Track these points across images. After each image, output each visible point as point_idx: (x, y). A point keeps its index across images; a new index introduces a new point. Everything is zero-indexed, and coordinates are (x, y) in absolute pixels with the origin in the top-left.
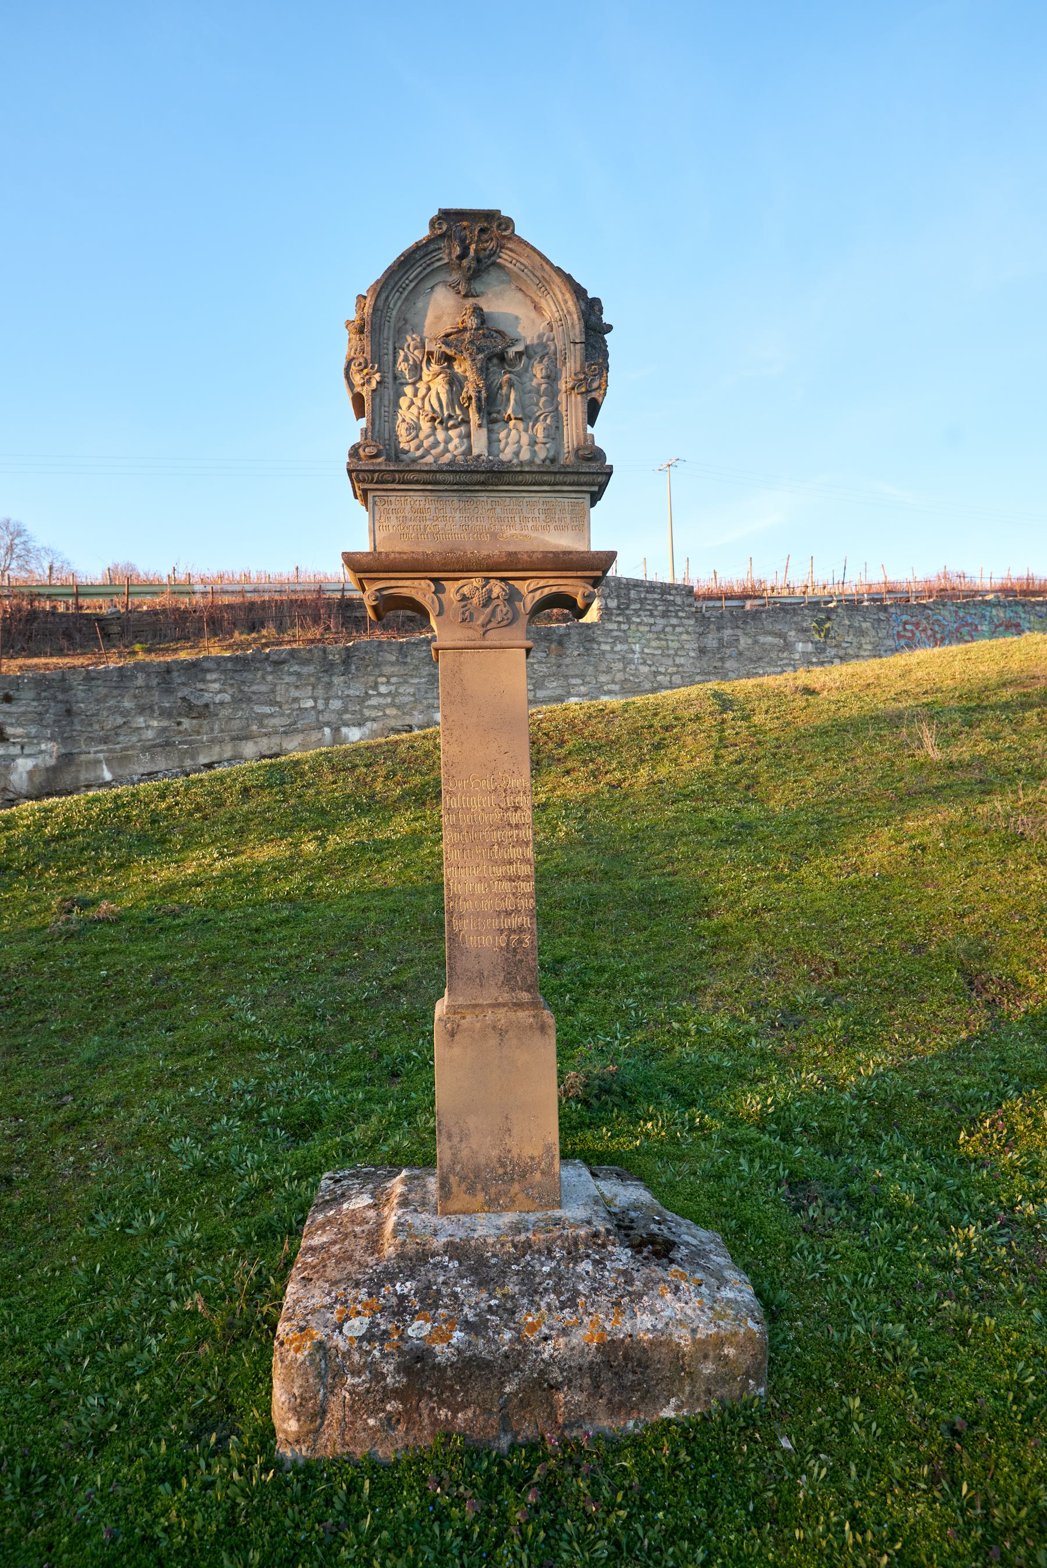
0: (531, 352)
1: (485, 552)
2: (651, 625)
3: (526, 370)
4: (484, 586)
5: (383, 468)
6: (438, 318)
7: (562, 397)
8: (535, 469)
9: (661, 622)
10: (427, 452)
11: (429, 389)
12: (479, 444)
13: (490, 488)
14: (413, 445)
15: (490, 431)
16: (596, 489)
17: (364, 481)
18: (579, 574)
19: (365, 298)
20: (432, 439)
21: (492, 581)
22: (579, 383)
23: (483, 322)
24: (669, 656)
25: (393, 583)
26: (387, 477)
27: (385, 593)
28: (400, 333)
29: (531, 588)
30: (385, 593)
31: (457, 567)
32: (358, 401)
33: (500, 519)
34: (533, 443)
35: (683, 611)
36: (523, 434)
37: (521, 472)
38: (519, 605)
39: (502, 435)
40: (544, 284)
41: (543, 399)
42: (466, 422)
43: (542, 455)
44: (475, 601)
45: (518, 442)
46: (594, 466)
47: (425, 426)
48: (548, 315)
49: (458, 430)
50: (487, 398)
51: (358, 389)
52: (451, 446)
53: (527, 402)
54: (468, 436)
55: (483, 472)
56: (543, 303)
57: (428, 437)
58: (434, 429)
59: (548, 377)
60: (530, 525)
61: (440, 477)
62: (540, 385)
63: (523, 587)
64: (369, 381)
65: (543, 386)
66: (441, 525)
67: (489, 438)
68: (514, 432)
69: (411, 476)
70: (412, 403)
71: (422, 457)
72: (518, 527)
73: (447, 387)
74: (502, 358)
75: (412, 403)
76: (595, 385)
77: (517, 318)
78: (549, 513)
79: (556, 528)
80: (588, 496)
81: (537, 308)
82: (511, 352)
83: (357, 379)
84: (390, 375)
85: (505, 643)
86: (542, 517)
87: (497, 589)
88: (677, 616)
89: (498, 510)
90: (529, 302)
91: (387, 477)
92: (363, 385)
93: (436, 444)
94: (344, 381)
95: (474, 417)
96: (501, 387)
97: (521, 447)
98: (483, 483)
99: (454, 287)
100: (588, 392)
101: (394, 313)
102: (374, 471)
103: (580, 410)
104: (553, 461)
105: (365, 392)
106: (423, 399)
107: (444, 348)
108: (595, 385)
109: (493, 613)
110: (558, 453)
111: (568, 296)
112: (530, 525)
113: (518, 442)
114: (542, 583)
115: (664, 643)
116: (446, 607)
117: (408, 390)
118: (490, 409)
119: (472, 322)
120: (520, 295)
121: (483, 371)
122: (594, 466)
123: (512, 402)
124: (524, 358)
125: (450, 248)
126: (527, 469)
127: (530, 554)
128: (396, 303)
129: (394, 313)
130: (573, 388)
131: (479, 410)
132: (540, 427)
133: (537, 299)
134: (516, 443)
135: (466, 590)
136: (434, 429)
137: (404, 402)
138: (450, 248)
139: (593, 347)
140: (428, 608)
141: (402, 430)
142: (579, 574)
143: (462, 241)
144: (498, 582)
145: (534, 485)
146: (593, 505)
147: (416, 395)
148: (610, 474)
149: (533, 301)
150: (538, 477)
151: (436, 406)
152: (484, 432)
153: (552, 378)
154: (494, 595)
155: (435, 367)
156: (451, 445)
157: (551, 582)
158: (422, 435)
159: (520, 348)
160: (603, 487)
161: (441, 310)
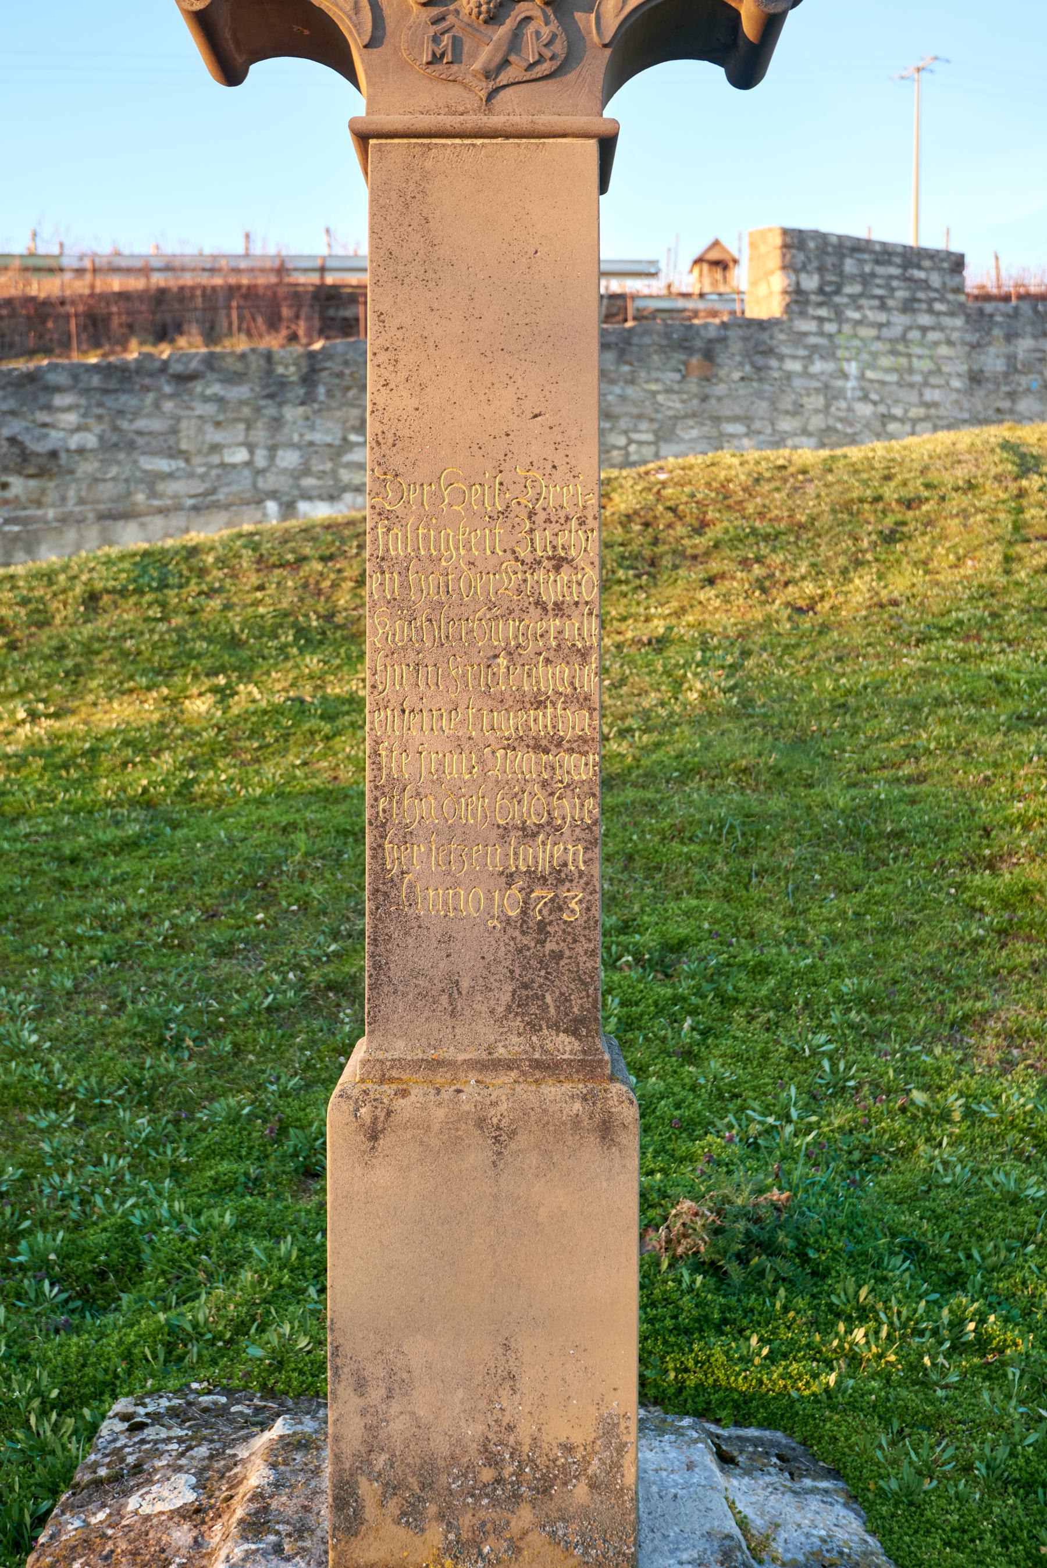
109: (515, 41)
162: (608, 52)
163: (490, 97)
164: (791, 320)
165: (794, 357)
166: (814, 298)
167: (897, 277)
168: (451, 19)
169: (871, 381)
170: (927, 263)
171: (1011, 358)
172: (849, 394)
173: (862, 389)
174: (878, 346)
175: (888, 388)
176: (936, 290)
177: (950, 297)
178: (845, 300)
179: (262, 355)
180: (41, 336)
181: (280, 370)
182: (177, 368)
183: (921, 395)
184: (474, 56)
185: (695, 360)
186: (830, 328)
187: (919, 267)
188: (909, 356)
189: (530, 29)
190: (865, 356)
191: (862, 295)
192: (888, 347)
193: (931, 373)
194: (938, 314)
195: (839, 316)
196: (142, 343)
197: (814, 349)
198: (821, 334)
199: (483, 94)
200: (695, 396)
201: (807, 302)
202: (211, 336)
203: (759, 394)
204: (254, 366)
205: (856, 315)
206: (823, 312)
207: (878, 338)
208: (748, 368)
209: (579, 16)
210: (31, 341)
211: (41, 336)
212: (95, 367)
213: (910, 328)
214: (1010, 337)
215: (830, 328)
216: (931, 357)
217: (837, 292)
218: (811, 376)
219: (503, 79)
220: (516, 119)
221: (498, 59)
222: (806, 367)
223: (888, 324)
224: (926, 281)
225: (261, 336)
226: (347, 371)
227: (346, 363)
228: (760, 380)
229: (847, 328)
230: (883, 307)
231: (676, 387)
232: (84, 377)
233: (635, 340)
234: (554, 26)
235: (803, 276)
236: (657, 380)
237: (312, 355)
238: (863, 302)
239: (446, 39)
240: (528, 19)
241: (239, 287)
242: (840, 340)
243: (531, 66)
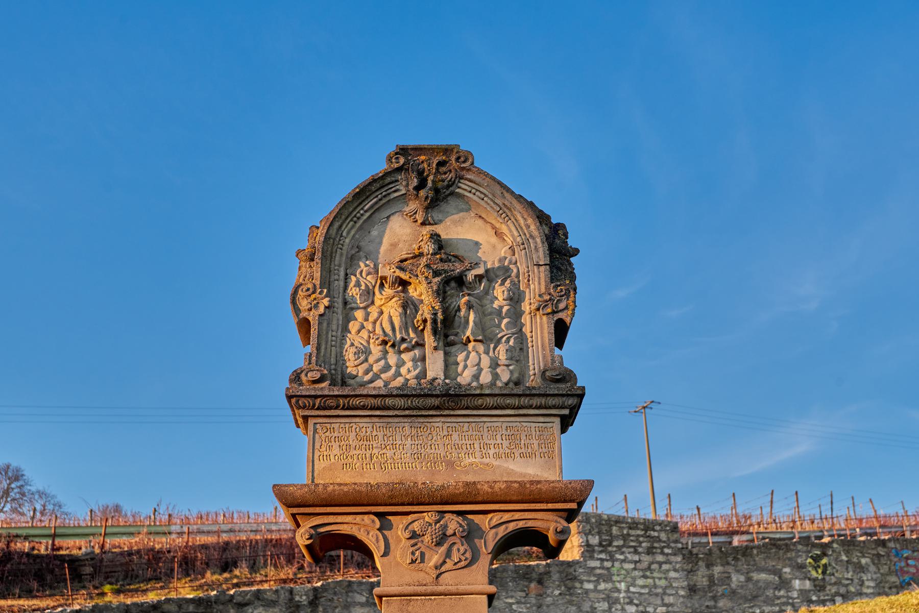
0: (492, 275)
3: (486, 292)
5: (326, 393)
6: (394, 245)
7: (526, 319)
8: (497, 392)
10: (377, 377)
12: (435, 367)
14: (361, 369)
15: (446, 354)
16: (566, 412)
17: (304, 407)
18: (550, 506)
19: (318, 228)
20: (382, 363)
21: (447, 516)
25: (331, 519)
27: (322, 530)
28: (352, 260)
29: (494, 523)
30: (322, 530)
31: (406, 500)
32: (304, 325)
34: (495, 364)
36: (483, 356)
38: (480, 543)
41: (505, 321)
42: (420, 345)
43: (505, 376)
44: (427, 538)
45: (478, 364)
46: (563, 387)
47: (376, 350)
48: (509, 240)
49: (412, 353)
50: (444, 321)
51: (304, 314)
54: (423, 359)
55: (437, 396)
60: (492, 452)
61: (389, 401)
62: (501, 307)
65: (505, 309)
66: (389, 453)
68: (473, 354)
69: (356, 402)
70: (363, 327)
71: (371, 381)
72: (478, 454)
73: (400, 310)
74: (460, 281)
75: (363, 327)
76: (562, 306)
79: (522, 455)
83: (304, 304)
84: (340, 300)
85: (462, 588)
86: (506, 443)
87: (453, 524)
89: (455, 436)
92: (310, 310)
93: (387, 368)
94: (289, 307)
95: (429, 339)
96: (459, 310)
97: (480, 370)
98: (437, 408)
100: (554, 312)
101: (347, 241)
102: (316, 397)
104: (517, 383)
105: (313, 317)
106: (375, 323)
107: (399, 273)
108: (562, 306)
109: (448, 554)
111: (530, 221)
112: (492, 452)
113: (478, 364)
114: (506, 517)
116: (392, 546)
117: (359, 314)
118: (446, 329)
120: (480, 222)
121: (441, 294)
123: (471, 323)
126: (487, 392)
129: (347, 241)
130: (538, 309)
131: (435, 332)
132: (502, 348)
133: (498, 225)
135: (416, 526)
137: (353, 326)
139: (559, 269)
140: (372, 547)
141: (349, 354)
142: (550, 506)
143: (420, 173)
144: (454, 517)
145: (496, 408)
147: (366, 320)
148: (581, 396)
149: (494, 227)
150: (500, 401)
151: (388, 330)
152: (440, 354)
153: (515, 299)
154: (450, 532)
155: (388, 291)
157: (517, 516)
158: (371, 359)
159: (480, 271)
160: (574, 410)
162: (490, 556)
163: (437, 577)
164: (585, 561)
165: (589, 581)
166: (596, 548)
167: (642, 536)
168: (419, 545)
169: (634, 593)
170: (658, 528)
171: (711, 578)
172: (622, 600)
173: (629, 598)
174: (636, 573)
175: (643, 597)
176: (664, 542)
177: (673, 545)
178: (614, 549)
179: (287, 590)
180: (155, 571)
181: (297, 598)
182: (239, 599)
183: (663, 600)
184: (430, 560)
185: (533, 585)
186: (608, 564)
187: (654, 530)
188: (653, 578)
189: (455, 548)
190: (629, 579)
191: (623, 546)
192: (641, 573)
193: (666, 587)
194: (667, 555)
195: (612, 559)
196: (213, 573)
197: (599, 576)
198: (602, 568)
199: (435, 576)
200: (534, 605)
201: (593, 551)
202: (253, 568)
203: (570, 603)
204: (282, 597)
205: (622, 557)
206: (603, 556)
207: (635, 569)
208: (563, 588)
209: (476, 540)
210: (149, 573)
211: (155, 571)
212: (192, 601)
213: (653, 563)
214: (709, 566)
215: (608, 564)
216: (666, 579)
217: (610, 545)
218: (600, 591)
219: (443, 569)
220: (450, 587)
221: (441, 561)
222: (596, 587)
223: (640, 561)
224: (658, 537)
225: (282, 567)
226: (335, 598)
227: (335, 593)
228: (571, 595)
229: (617, 564)
230: (636, 552)
231: (523, 600)
232: (185, 606)
233: (499, 575)
234: (466, 546)
235: (590, 537)
236: (512, 597)
237: (315, 589)
238: (624, 549)
239: (417, 553)
240: (454, 543)
241: (271, 540)
242: (614, 570)
243: (456, 564)
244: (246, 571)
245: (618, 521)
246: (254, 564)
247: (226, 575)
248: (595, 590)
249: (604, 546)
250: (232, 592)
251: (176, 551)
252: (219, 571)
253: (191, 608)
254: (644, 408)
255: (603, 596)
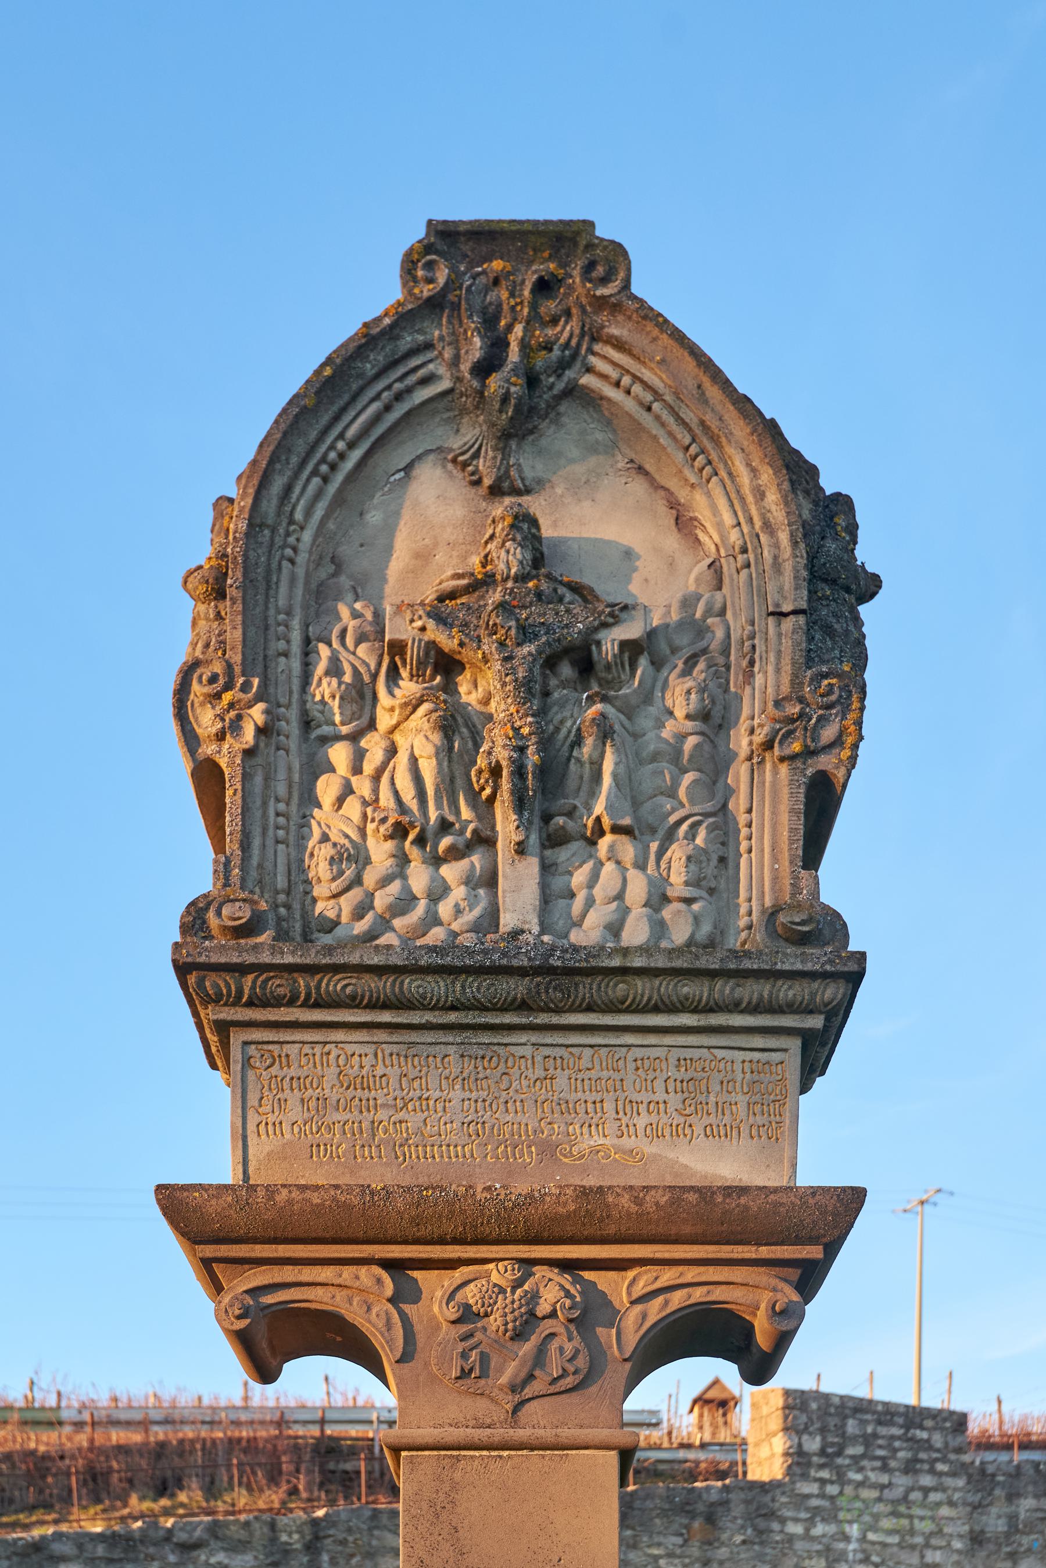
0: (664, 648)
1: (521, 1187)
2: (882, 1487)
3: (647, 697)
4: (518, 1284)
5: (266, 958)
6: (423, 557)
7: (739, 774)
8: (661, 962)
9: (902, 1481)
10: (384, 924)
11: (392, 751)
12: (518, 904)
13: (542, 1019)
14: (347, 903)
15: (547, 868)
16: (816, 1022)
17: (216, 999)
18: (764, 1252)
19: (231, 501)
20: (395, 887)
21: (540, 1271)
22: (787, 727)
23: (538, 561)
24: (913, 1547)
25: (288, 1274)
26: (279, 986)
27: (269, 1299)
28: (320, 599)
29: (639, 1290)
30: (269, 1299)
31: (449, 1229)
32: (208, 779)
33: (566, 1107)
34: (658, 899)
35: (944, 1460)
36: (632, 874)
37: (624, 971)
38: (606, 1335)
39: (579, 878)
40: (703, 447)
41: (688, 778)
42: (485, 840)
43: (680, 934)
44: (495, 1322)
45: (620, 896)
46: (815, 958)
47: (380, 852)
48: (710, 538)
49: (464, 864)
50: (542, 770)
51: (208, 749)
52: (445, 909)
53: (647, 786)
54: (490, 880)
55: (522, 972)
56: (700, 506)
57: (385, 882)
58: (403, 860)
59: (703, 716)
60: (641, 1121)
61: (412, 985)
62: (682, 737)
63: (616, 1287)
64: (236, 726)
65: (692, 741)
66: (414, 1120)
67: (544, 887)
68: (609, 867)
69: (336, 985)
70: (348, 790)
71: (370, 936)
72: (611, 1127)
73: (437, 738)
74: (585, 664)
75: (348, 790)
76: (828, 733)
77: (628, 554)
78: (691, 1090)
79: (709, 1132)
80: (795, 1045)
81: (684, 523)
82: (610, 641)
83: (206, 720)
84: (293, 714)
85: (567, 1433)
86: (674, 1100)
87: (552, 1291)
88: (932, 1471)
89: (562, 1081)
90: (661, 507)
91: (279, 986)
92: (220, 737)
93: (405, 903)
94: (172, 728)
95: (506, 825)
96: (578, 742)
97: (626, 911)
98: (523, 1006)
99: (462, 463)
100: (809, 753)
101: (307, 536)
102: (242, 969)
103: (784, 807)
104: (711, 945)
105: (227, 756)
106: (376, 778)
107: (436, 634)
108: (828, 733)
109: (540, 1357)
110: (720, 930)
111: (766, 475)
112: (641, 1121)
113: (620, 896)
114: (668, 1276)
115: (905, 1522)
116: (421, 1340)
117: (339, 754)
118: (547, 795)
119: (509, 559)
120: (638, 487)
121: (534, 692)
122: (815, 958)
123: (607, 780)
124: (643, 662)
125: (455, 343)
126: (638, 962)
127: (639, 1194)
128: (310, 507)
129: (307, 536)
130: (768, 745)
131: (520, 803)
132: (677, 853)
133: (683, 495)
134: (617, 897)
135: (471, 1294)
136: (403, 860)
137: (327, 789)
138: (455, 343)
139: (829, 631)
140: (378, 1341)
141: (319, 865)
142: (764, 1252)
143: (490, 320)
144: (553, 1273)
145: (656, 1009)
146: (805, 1088)
147: (357, 770)
148: (855, 978)
149: (674, 504)
150: (666, 987)
151: (413, 804)
152: (531, 866)
153: (714, 719)
154: (543, 1308)
155: (408, 688)
156: (444, 904)
157: (691, 1274)
158: (370, 878)
159: (631, 630)
160: (837, 1016)
161: (430, 529)
162: (628, 1366)
163: (516, 1409)
164: (793, 1483)
165: (796, 1520)
166: (815, 1459)
167: (899, 1438)
168: (479, 1336)
169: (873, 1543)
170: (929, 1423)
171: (1012, 1519)
172: (851, 1556)
173: (864, 1551)
174: (879, 1508)
175: (889, 1550)
176: (938, 1450)
177: (952, 1457)
178: (847, 1461)
179: (265, 1523)
180: (41, 1491)
181: (284, 1538)
182: (182, 1536)
183: (922, 1557)
184: (501, 1371)
185: (696, 1524)
186: (832, 1490)
187: (922, 1428)
188: (911, 1517)
189: (554, 1345)
190: (867, 1518)
191: (863, 1456)
192: (889, 1508)
193: (931, 1534)
194: (941, 1474)
195: (841, 1479)
196: (142, 1499)
197: (816, 1511)
198: (822, 1496)
199: (509, 1407)
200: (697, 1560)
201: (809, 1464)
202: (212, 1490)
203: (760, 1557)
204: (258, 1533)
205: (859, 1477)
206: (825, 1474)
207: (880, 1499)
208: (749, 1531)
209: (600, 1331)
210: (31, 1496)
211: (41, 1491)
212: (100, 1537)
213: (912, 1489)
214: (1012, 1497)
215: (832, 1490)
216: (933, 1518)
217: (839, 1453)
218: (813, 1539)
219: (528, 1392)
220: (541, 1432)
221: (523, 1375)
222: (807, 1530)
223: (890, 1485)
224: (928, 1441)
225: (261, 1490)
226: (351, 1539)
227: (349, 1530)
228: (762, 1543)
229: (849, 1490)
230: (885, 1468)
231: (678, 1551)
232: (89, 1547)
233: (637, 1504)
234: (577, 1342)
235: (805, 1437)
236: (659, 1545)
237: (315, 1522)
238: (864, 1463)
239: (474, 1355)
240: (553, 1335)
241: (239, 1440)
242: (842, 1502)
243: (555, 1380)
244: (198, 1495)
245: (860, 1407)
246: (212, 1482)
247: (164, 1502)
248: (807, 1536)
249: (829, 1455)
250: (170, 1523)
251: (73, 1457)
252: (151, 1494)
253: (100, 1550)
254: (922, 1203)
255: (819, 1547)
